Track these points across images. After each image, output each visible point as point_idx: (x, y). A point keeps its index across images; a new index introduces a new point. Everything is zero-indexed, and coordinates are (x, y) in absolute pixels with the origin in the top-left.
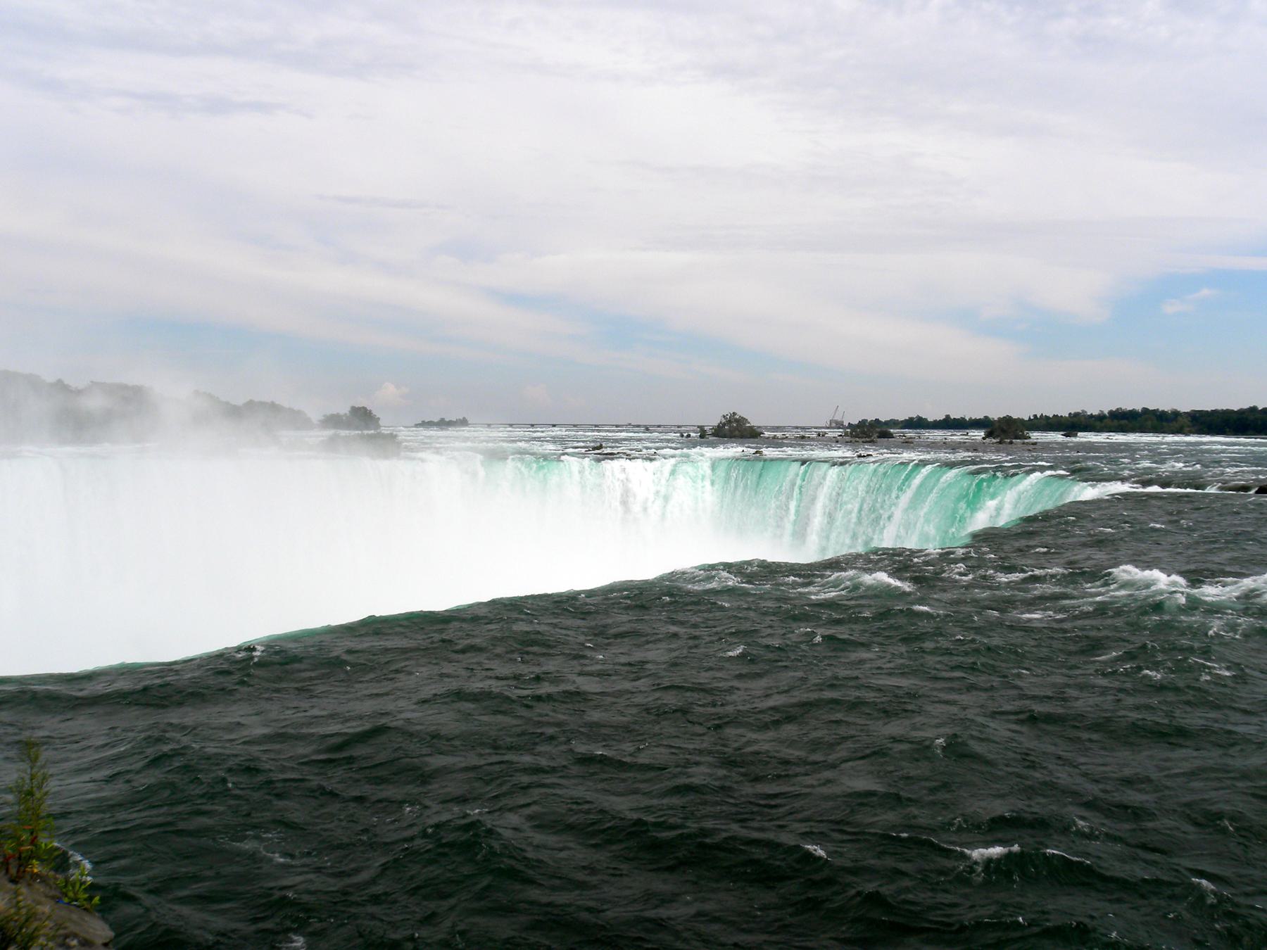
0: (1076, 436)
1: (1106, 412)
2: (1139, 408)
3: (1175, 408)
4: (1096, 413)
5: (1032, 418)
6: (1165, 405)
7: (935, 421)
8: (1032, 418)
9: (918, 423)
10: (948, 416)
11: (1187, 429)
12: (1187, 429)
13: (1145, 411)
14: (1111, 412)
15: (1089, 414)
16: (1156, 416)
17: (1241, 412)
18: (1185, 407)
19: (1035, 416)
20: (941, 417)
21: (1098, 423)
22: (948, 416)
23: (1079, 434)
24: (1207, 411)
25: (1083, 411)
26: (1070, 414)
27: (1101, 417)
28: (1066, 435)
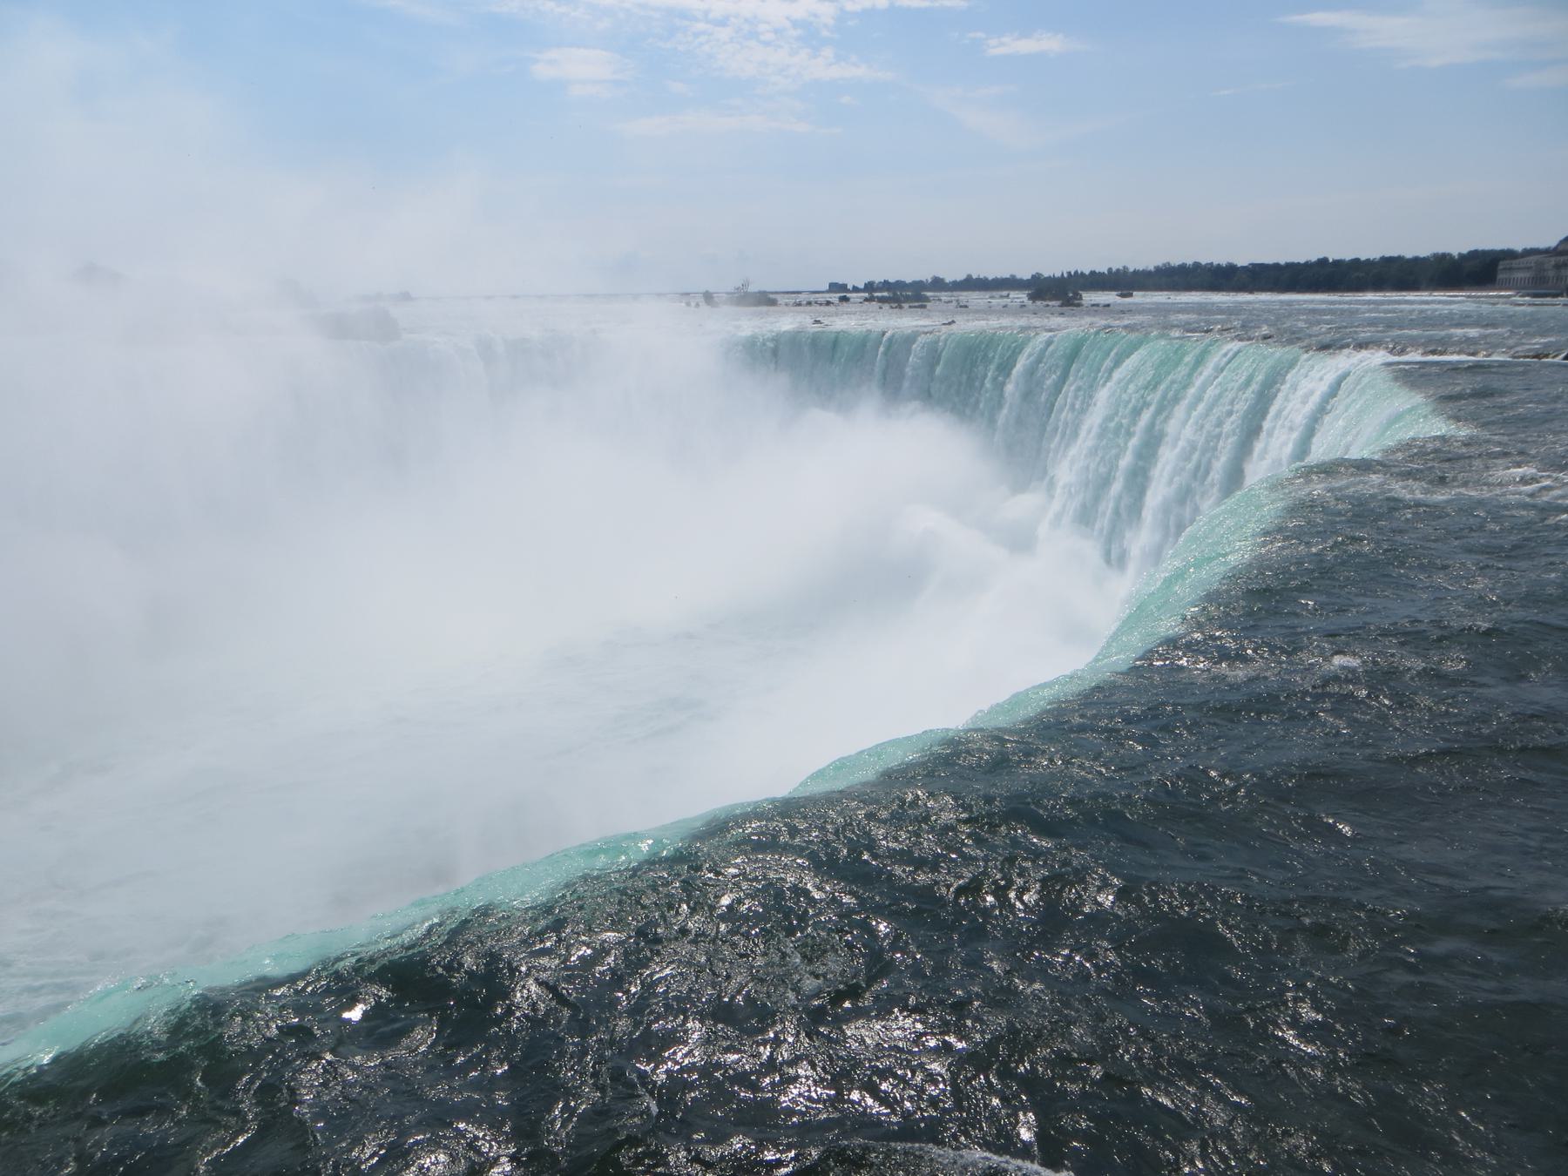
3: (1230, 261)
5: (1065, 275)
6: (1220, 258)
8: (1065, 275)
9: (938, 284)
13: (1197, 265)
15: (1131, 270)
17: (1308, 265)
18: (1242, 261)
19: (1069, 273)
20: (961, 277)
24: (1276, 266)
25: (1124, 267)
26: (1110, 270)
28: (1123, 296)
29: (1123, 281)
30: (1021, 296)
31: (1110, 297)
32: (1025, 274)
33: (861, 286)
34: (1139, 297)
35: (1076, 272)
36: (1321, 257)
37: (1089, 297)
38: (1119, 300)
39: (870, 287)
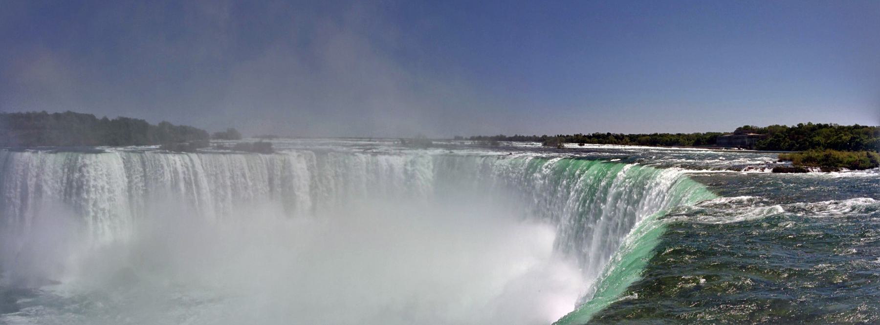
0: (584, 145)
1: (591, 135)
2: (606, 133)
4: (587, 134)
7: (510, 137)
9: (502, 138)
10: (516, 135)
11: (629, 143)
12: (629, 143)
13: (609, 134)
14: (593, 134)
15: (583, 135)
16: (614, 136)
19: (558, 136)
20: (513, 135)
21: (588, 140)
22: (516, 135)
23: (585, 144)
27: (589, 137)
28: (580, 145)
29: (581, 140)
30: (540, 145)
31: (576, 146)
32: (540, 136)
33: (469, 138)
34: (587, 146)
35: (561, 136)
36: (656, 132)
37: (566, 145)
38: (579, 147)
39: (472, 139)
